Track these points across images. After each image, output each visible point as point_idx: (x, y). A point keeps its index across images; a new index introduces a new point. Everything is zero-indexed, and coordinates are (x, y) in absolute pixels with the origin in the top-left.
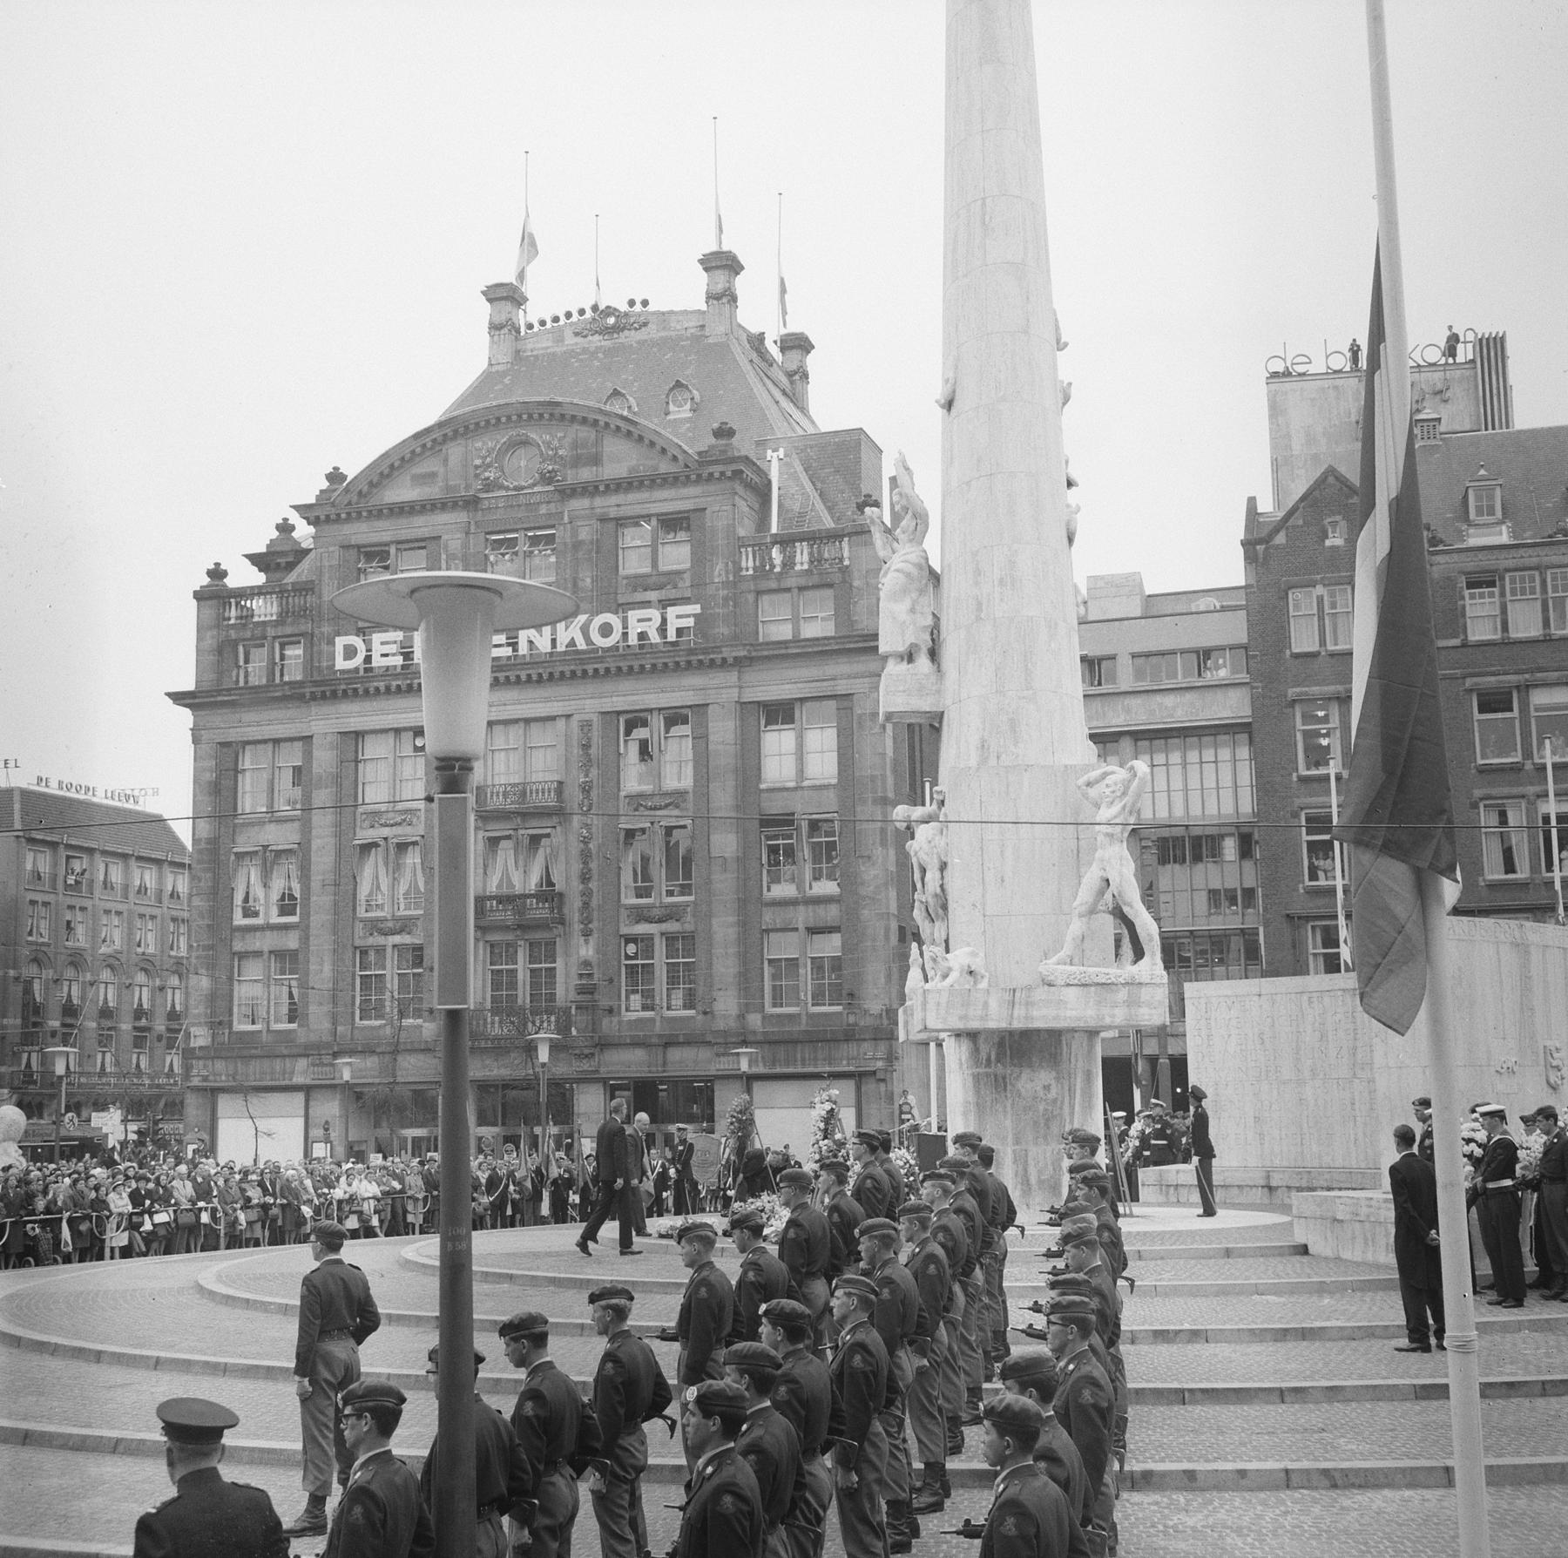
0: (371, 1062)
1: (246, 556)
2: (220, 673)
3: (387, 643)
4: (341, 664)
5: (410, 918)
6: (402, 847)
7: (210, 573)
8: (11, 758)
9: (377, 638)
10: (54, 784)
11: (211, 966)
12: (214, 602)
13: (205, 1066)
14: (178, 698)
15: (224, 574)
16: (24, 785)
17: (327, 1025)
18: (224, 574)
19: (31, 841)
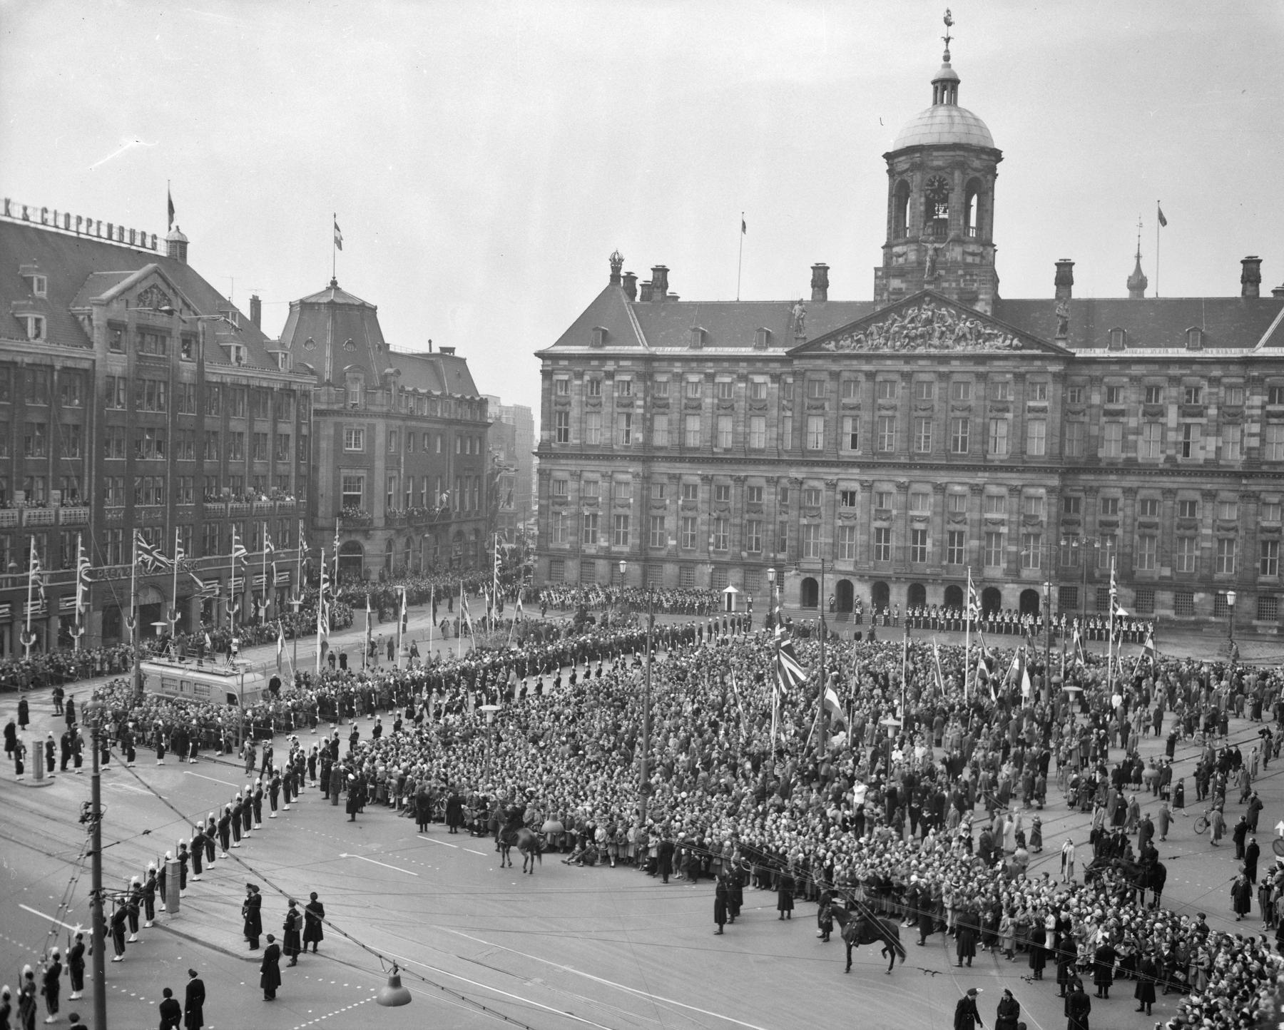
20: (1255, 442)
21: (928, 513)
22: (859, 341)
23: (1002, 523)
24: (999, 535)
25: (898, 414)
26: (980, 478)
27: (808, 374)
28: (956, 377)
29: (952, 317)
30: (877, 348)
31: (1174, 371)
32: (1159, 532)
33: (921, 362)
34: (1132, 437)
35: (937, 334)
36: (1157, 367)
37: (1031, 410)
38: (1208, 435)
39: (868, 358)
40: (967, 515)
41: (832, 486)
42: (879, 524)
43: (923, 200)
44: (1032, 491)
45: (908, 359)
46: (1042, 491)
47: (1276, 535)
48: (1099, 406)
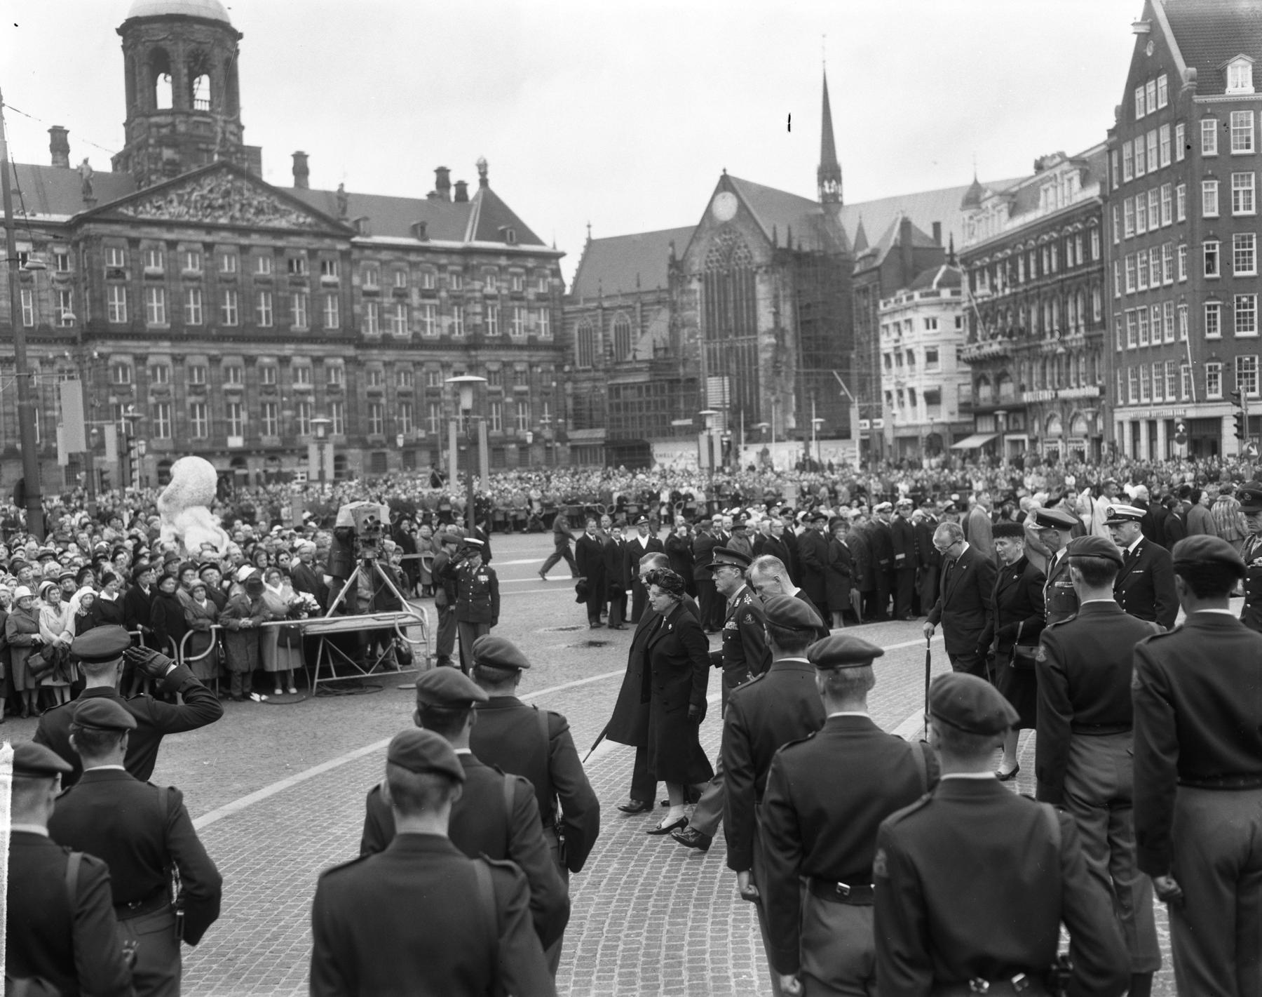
20: (478, 320)
21: (240, 387)
22: (159, 208)
23: (307, 392)
24: (306, 404)
25: (203, 285)
26: (288, 349)
27: (105, 240)
28: (255, 250)
29: (249, 190)
30: (179, 215)
31: (413, 257)
32: (412, 400)
33: (224, 234)
34: (387, 316)
35: (238, 206)
36: (398, 254)
37: (326, 285)
38: (441, 314)
39: (169, 225)
40: (278, 387)
41: (141, 359)
42: (192, 399)
43: (185, 71)
44: (330, 361)
45: (210, 228)
46: (340, 361)
47: (498, 397)
48: (359, 287)
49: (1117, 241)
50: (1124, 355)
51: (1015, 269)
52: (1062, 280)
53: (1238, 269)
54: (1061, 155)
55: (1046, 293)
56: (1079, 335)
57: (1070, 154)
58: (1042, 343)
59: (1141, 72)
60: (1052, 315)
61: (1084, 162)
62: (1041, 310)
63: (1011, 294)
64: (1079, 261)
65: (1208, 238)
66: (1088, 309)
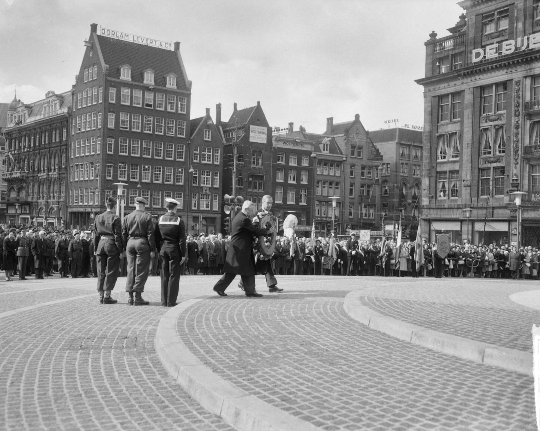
0: (484, 211)
1: (448, 30)
2: (433, 71)
3: (493, 49)
4: (475, 60)
5: (500, 157)
6: (497, 130)
7: (431, 35)
8: (396, 119)
9: (488, 48)
10: (410, 126)
11: (430, 177)
12: (432, 45)
13: (427, 212)
14: (419, 82)
15: (436, 35)
16: (400, 127)
17: (468, 197)
18: (436, 35)
19: (401, 144)
49: (73, 134)
50: (73, 183)
51: (30, 141)
52: (49, 148)
53: (121, 152)
54: (53, 92)
55: (42, 153)
56: (55, 173)
57: (57, 92)
58: (39, 175)
59: (87, 63)
60: (44, 163)
61: (63, 97)
62: (40, 160)
63: (27, 151)
64: (57, 141)
65: (110, 137)
66: (60, 161)
